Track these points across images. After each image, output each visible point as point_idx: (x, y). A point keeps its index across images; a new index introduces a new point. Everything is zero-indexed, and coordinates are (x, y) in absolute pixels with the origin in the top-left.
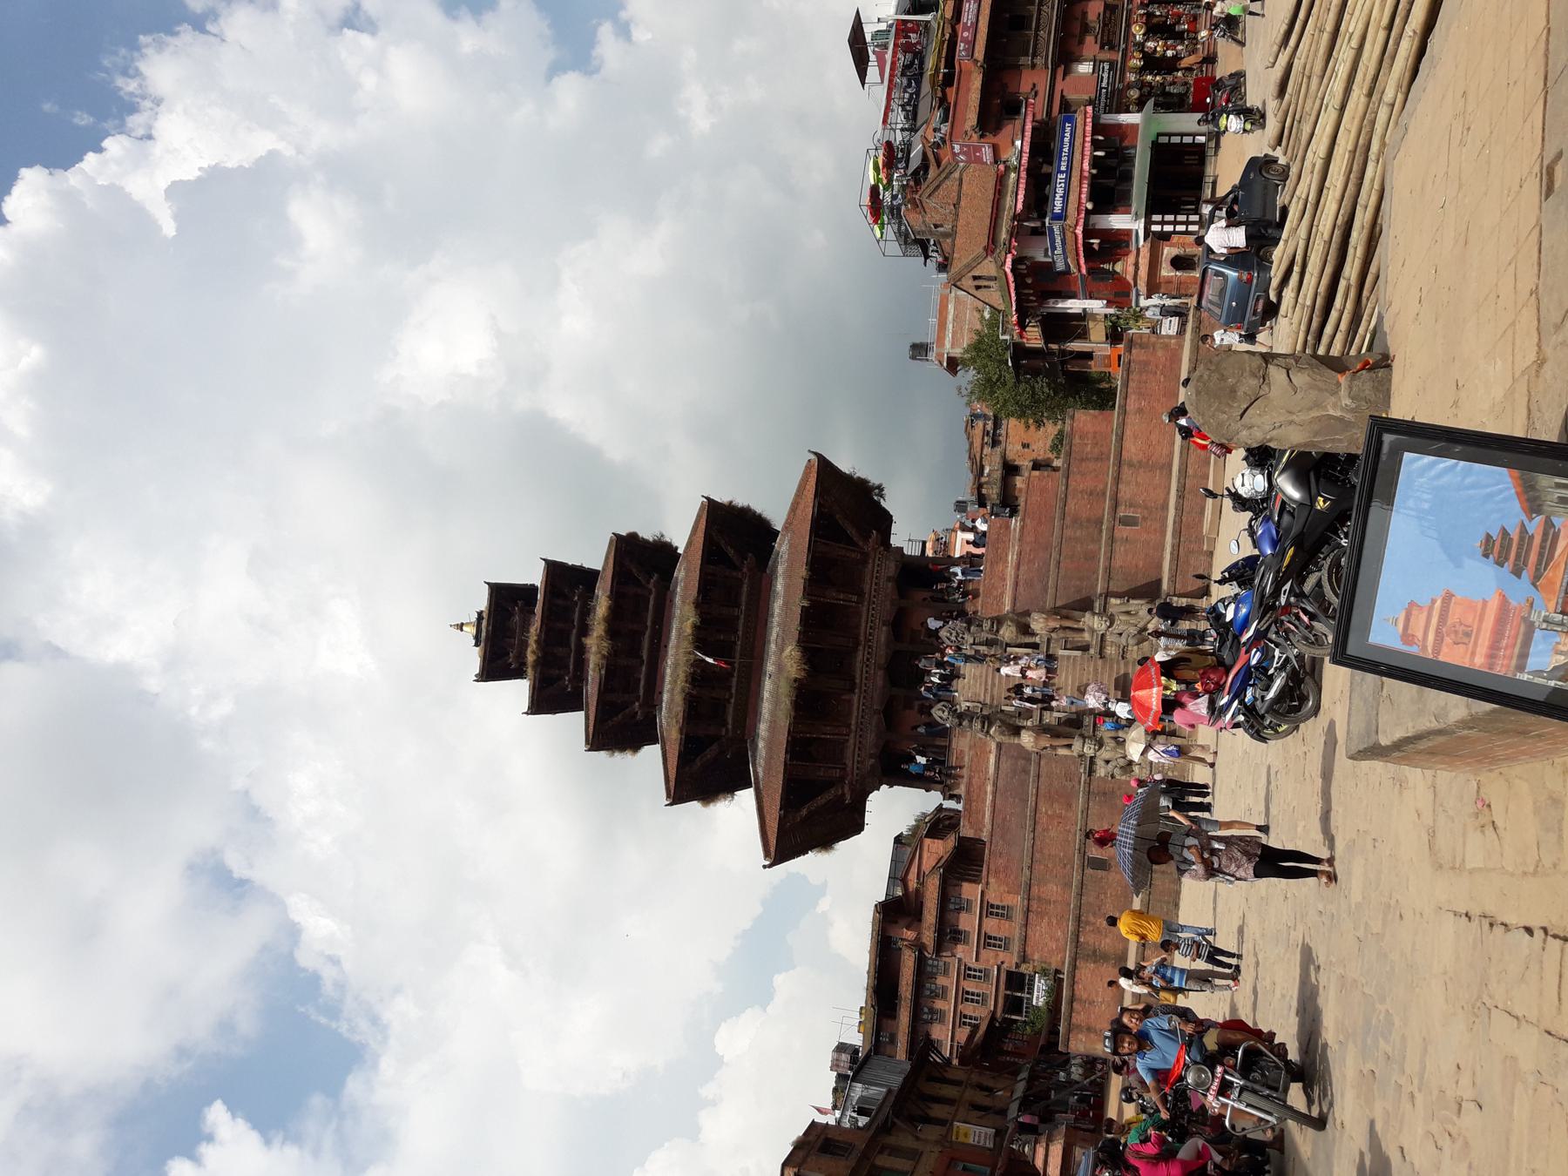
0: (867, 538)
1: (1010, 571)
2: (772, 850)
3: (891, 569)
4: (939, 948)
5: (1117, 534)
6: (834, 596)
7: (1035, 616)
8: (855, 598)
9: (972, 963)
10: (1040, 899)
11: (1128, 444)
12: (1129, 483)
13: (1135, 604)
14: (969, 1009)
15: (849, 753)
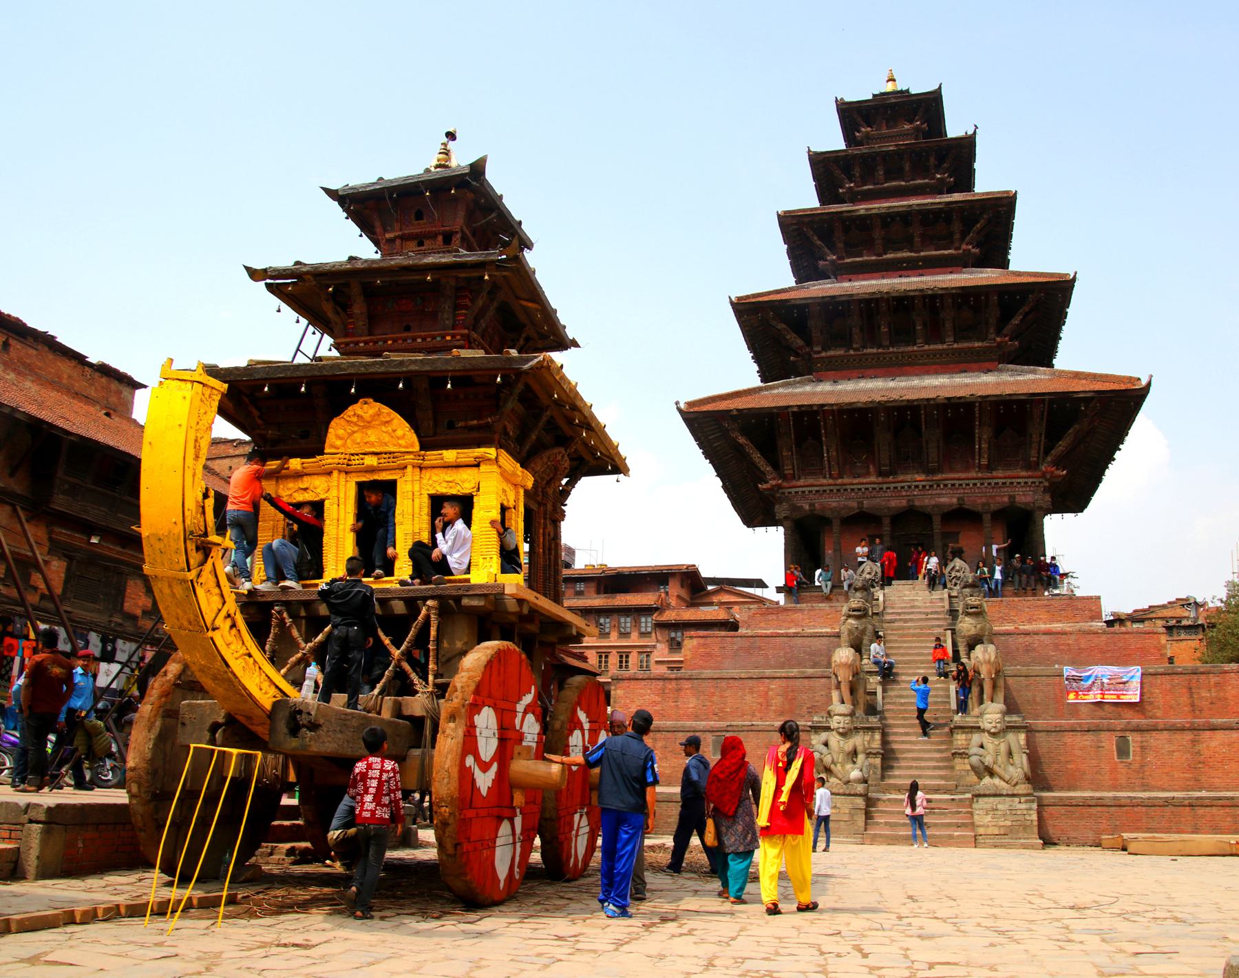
0: (1058, 463)
1: (1043, 627)
2: (696, 409)
3: (1025, 497)
4: (660, 626)
5: (1104, 735)
6: (983, 436)
7: (991, 648)
8: (984, 462)
9: (655, 657)
10: (679, 690)
11: (1220, 735)
12: (1170, 741)
13: (1021, 760)
14: (614, 659)
15: (810, 481)
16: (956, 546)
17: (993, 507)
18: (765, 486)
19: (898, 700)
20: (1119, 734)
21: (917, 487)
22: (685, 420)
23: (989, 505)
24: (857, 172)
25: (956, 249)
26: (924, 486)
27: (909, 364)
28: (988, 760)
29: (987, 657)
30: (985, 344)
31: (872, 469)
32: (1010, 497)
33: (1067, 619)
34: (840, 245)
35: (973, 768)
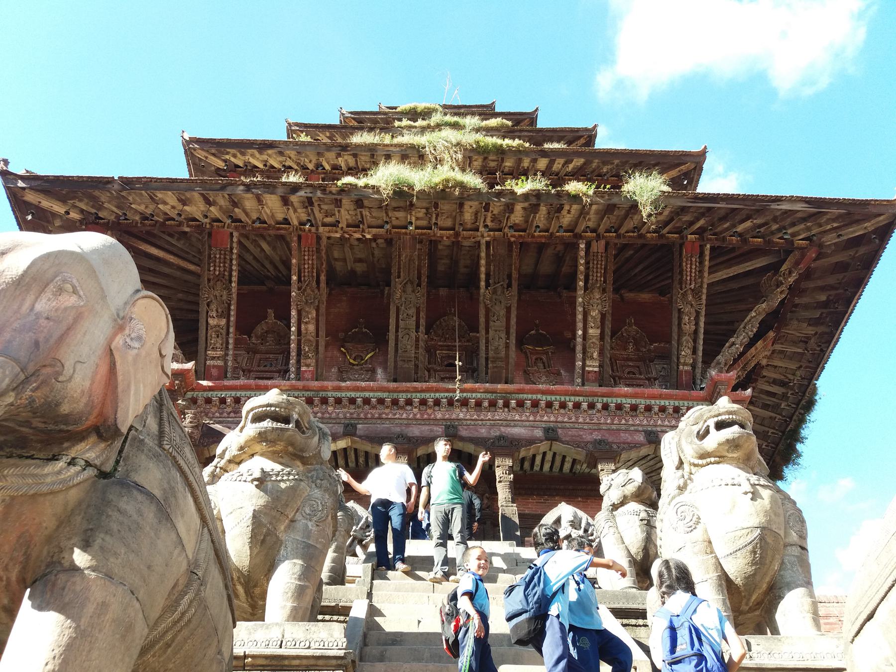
8: (593, 366)
23: (608, 443)
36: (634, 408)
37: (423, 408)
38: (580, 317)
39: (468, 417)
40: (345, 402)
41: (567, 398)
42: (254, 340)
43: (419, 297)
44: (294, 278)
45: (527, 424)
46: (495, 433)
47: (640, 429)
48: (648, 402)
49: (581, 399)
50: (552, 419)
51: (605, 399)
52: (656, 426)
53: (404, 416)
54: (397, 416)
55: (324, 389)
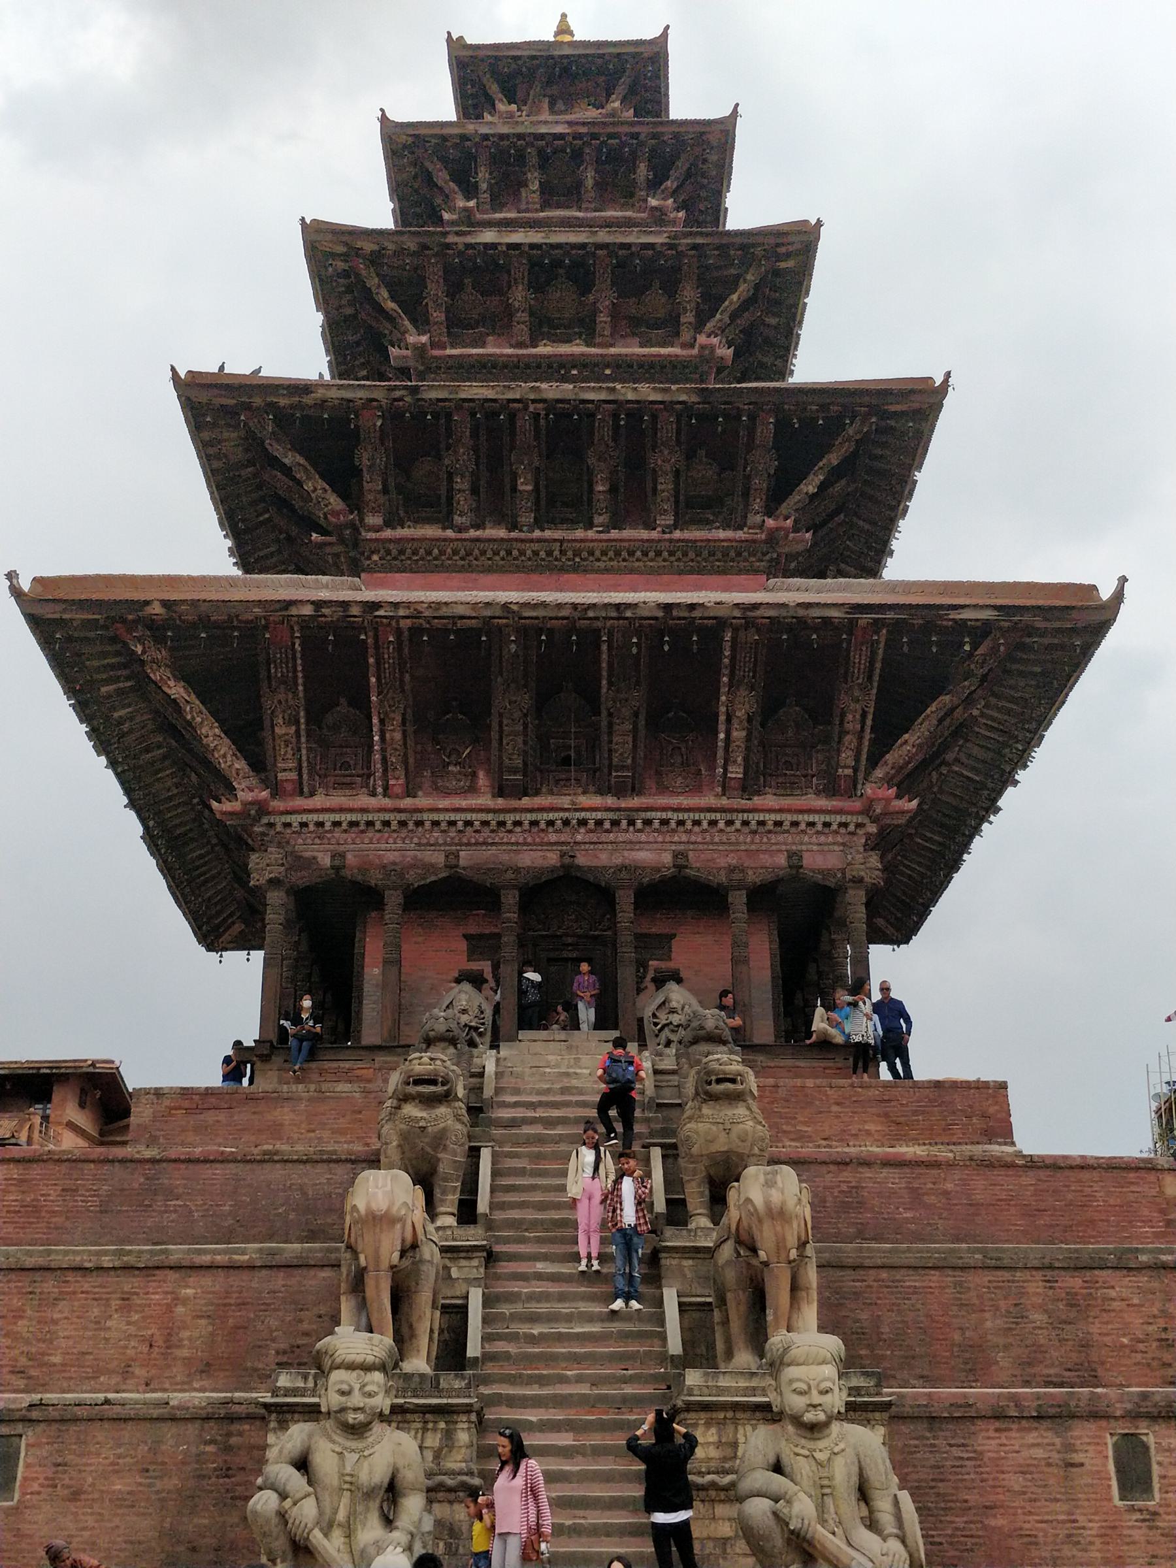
5: (1082, 1432)
8: (736, 772)
16: (663, 965)
17: (752, 877)
18: (227, 806)
19: (523, 1329)
20: (1123, 1428)
21: (583, 823)
22: (36, 622)
24: (483, 177)
25: (684, 346)
26: (599, 823)
27: (575, 569)
28: (802, 1509)
29: (775, 1197)
30: (740, 534)
31: (482, 779)
32: (791, 855)
33: (929, 1136)
34: (438, 316)
35: (748, 1532)
36: (778, 824)
37: (535, 829)
38: (722, 718)
39: (587, 840)
40: (444, 825)
41: (702, 815)
42: (325, 731)
43: (525, 700)
44: (373, 680)
45: (655, 846)
46: (617, 860)
47: (784, 847)
48: (795, 818)
49: (718, 815)
50: (684, 838)
51: (745, 815)
52: (802, 844)
53: (513, 840)
54: (505, 840)
55: (420, 811)
